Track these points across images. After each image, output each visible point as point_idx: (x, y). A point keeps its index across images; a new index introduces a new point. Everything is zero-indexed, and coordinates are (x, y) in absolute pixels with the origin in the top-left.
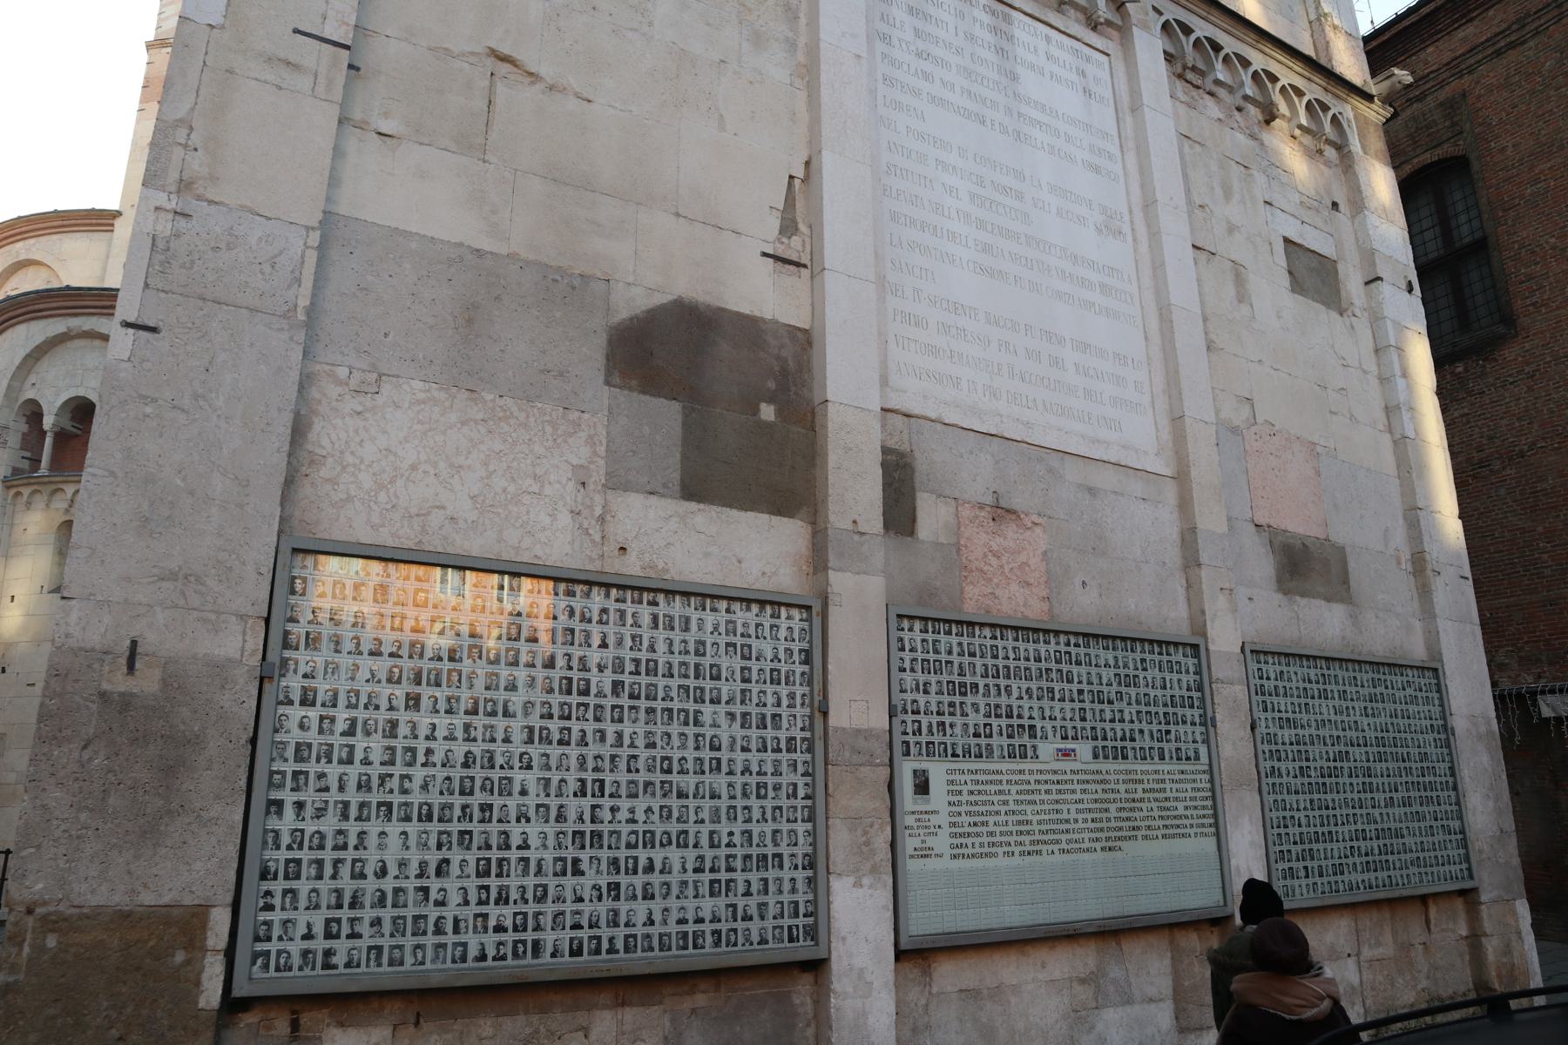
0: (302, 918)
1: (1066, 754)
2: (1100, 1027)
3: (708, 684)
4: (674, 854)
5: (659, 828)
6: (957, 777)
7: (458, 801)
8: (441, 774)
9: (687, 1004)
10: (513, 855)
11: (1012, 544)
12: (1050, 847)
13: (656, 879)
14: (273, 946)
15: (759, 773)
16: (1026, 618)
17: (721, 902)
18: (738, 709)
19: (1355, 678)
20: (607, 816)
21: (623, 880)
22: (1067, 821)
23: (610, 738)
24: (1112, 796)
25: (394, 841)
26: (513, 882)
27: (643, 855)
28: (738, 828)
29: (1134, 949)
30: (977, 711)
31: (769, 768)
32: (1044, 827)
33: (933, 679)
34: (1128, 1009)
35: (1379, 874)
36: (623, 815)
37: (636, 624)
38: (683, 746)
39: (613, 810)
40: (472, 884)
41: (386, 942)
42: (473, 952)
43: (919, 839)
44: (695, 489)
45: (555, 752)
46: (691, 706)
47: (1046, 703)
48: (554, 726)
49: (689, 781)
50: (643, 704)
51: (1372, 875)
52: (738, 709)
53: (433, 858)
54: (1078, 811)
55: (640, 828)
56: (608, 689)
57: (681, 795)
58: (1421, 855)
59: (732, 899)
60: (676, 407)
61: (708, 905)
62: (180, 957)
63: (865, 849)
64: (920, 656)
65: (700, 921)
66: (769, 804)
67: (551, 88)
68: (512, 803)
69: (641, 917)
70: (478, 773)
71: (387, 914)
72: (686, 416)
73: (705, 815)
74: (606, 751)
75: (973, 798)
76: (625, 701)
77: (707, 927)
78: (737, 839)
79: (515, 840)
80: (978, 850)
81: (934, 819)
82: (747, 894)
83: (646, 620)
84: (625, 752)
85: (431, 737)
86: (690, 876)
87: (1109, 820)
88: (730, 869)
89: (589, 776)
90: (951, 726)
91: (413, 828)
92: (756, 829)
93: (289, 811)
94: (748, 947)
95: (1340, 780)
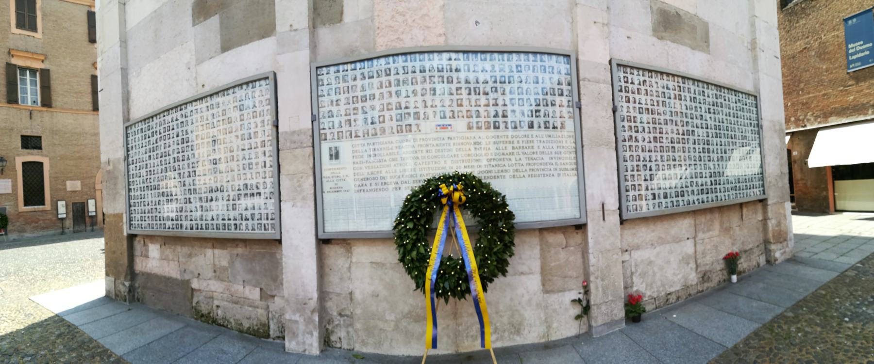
15: (249, 159)
31: (253, 156)
35: (710, 195)
51: (705, 196)
53: (157, 199)
63: (298, 189)
65: (229, 219)
80: (374, 187)
90: (355, 121)
91: (153, 192)
94: (247, 231)
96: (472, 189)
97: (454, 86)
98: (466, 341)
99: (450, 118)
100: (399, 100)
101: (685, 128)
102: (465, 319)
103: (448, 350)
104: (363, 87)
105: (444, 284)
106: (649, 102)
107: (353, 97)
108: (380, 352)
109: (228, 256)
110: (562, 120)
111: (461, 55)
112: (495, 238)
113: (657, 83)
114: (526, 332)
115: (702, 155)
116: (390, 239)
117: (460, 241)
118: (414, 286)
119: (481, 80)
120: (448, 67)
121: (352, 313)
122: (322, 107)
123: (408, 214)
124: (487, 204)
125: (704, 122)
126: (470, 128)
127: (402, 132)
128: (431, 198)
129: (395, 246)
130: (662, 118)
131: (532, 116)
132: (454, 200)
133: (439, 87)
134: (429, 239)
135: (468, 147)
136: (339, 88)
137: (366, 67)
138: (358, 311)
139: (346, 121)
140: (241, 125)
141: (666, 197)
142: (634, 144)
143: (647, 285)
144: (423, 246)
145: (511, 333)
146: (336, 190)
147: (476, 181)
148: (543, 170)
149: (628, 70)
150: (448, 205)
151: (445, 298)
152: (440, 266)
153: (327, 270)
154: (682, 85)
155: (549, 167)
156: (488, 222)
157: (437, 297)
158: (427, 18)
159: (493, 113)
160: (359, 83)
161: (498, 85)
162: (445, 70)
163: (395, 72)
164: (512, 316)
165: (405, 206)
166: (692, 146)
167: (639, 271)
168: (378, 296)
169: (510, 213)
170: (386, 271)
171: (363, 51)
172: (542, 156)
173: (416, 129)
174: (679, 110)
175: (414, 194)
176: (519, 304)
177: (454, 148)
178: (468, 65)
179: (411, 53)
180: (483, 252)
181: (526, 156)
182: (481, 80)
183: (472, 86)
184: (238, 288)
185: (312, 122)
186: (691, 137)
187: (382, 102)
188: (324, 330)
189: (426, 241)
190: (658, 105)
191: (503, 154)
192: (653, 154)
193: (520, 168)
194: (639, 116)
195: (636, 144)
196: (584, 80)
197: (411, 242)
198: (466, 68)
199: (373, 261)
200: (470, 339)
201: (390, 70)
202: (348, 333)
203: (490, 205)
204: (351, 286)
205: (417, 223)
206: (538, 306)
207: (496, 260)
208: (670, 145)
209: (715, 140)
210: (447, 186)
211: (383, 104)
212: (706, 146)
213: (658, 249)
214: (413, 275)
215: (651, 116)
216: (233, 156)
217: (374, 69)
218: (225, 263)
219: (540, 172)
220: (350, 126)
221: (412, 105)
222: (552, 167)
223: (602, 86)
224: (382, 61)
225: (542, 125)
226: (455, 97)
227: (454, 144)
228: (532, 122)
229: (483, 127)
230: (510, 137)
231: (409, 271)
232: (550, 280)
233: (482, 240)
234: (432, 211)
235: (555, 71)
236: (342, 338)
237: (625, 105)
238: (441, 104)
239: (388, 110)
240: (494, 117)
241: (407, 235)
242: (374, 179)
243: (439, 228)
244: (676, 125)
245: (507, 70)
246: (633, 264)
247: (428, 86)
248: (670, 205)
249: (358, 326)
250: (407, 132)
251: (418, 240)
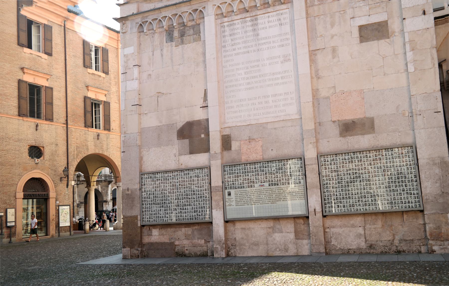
0: (147, 216)
1: (262, 186)
2: (274, 236)
3: (192, 182)
4: (189, 207)
5: (186, 204)
7: (161, 202)
8: (159, 199)
9: (194, 228)
10: (168, 208)
11: (253, 146)
12: (258, 203)
13: (186, 210)
14: (144, 220)
16: (257, 160)
17: (196, 213)
18: (197, 185)
19: (367, 155)
20: (179, 202)
21: (182, 211)
22: (262, 198)
23: (179, 192)
24: (274, 193)
25: (155, 207)
26: (168, 212)
27: (184, 207)
28: (198, 203)
29: (283, 223)
30: (241, 180)
31: (202, 194)
32: (256, 200)
33: (231, 175)
34: (281, 234)
36: (181, 202)
37: (182, 175)
38: (189, 192)
39: (180, 201)
40: (164, 212)
41: (155, 219)
42: (165, 220)
44: (192, 152)
45: (172, 194)
46: (190, 186)
47: (257, 177)
48: (172, 191)
49: (190, 197)
50: (183, 186)
52: (197, 185)
53: (159, 209)
54: (265, 196)
55: (184, 204)
56: (178, 185)
57: (189, 199)
59: (197, 213)
60: (188, 140)
61: (194, 214)
62: (136, 221)
64: (229, 172)
65: (193, 216)
66: (202, 199)
67: (166, 94)
68: (168, 202)
69: (185, 216)
70: (163, 198)
71: (155, 216)
72: (189, 141)
73: (193, 201)
74: (179, 194)
75: (240, 195)
76: (181, 186)
77: (194, 217)
78: (198, 204)
79: (168, 206)
80: (241, 204)
81: (232, 200)
82: (200, 212)
83: (183, 175)
84: (181, 193)
85: (158, 194)
86: (191, 210)
87: (273, 197)
88: (197, 209)
89: (177, 197)
91: (157, 206)
92: (200, 203)
93: (144, 205)
109: (191, 230)
133: (260, 173)
135: (269, 191)
141: (344, 207)
143: (338, 243)
155: (295, 197)
167: (334, 237)
213: (343, 229)
218: (190, 233)
222: (296, 197)
226: (265, 176)
245: (280, 165)
246: (331, 233)
247: (257, 173)
248: (346, 210)
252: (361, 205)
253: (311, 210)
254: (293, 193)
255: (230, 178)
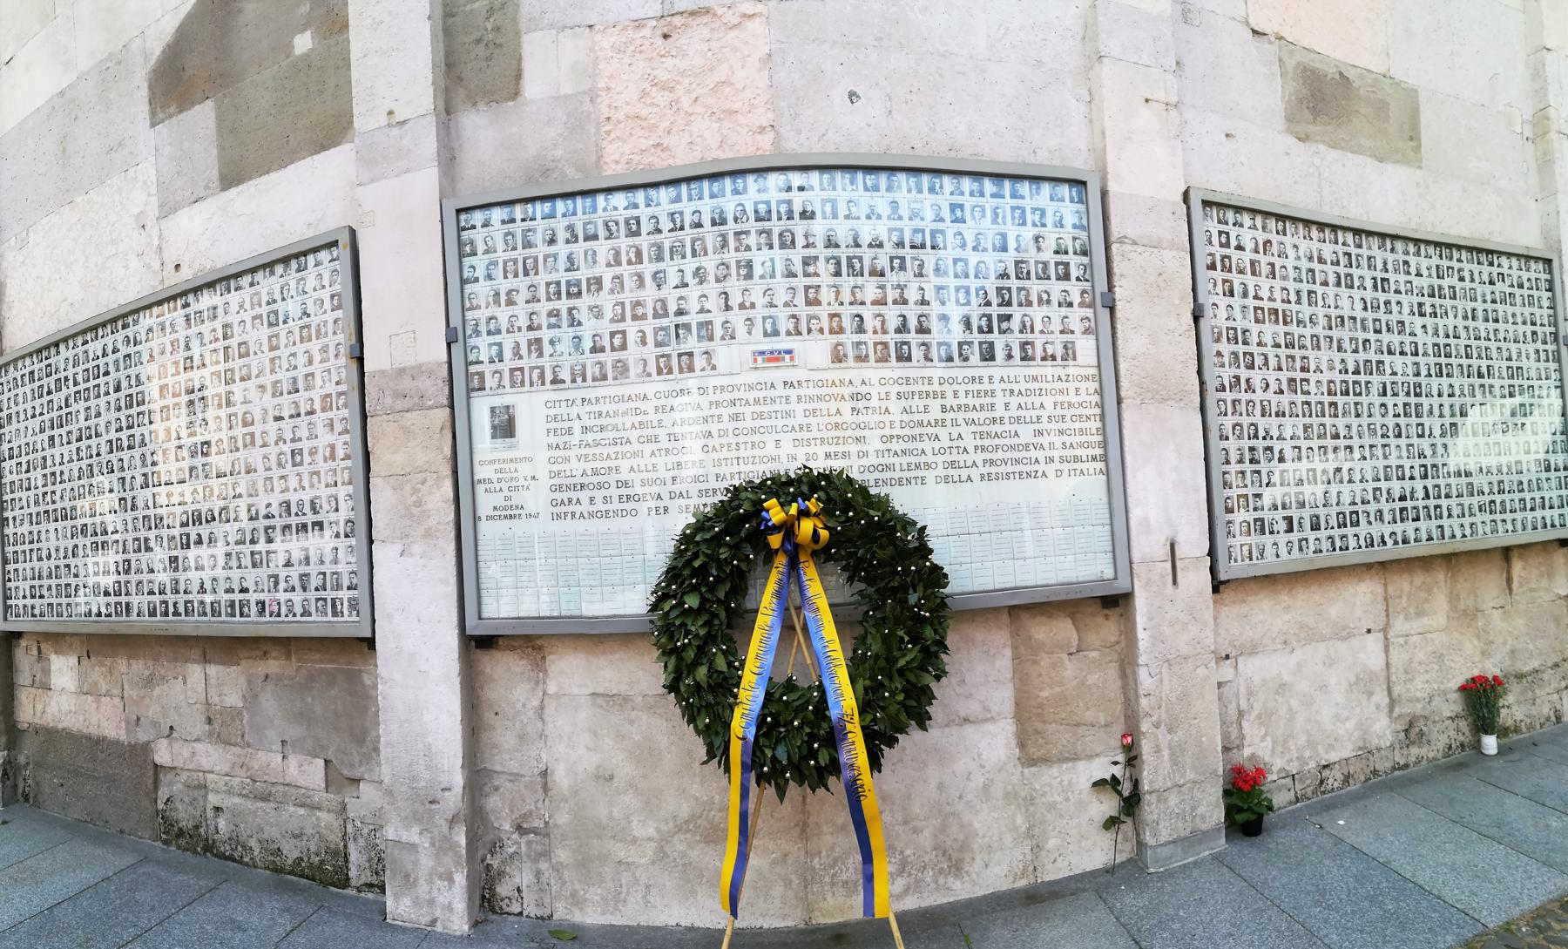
6: (563, 410)
15: (293, 440)
43: (501, 495)
58: (1498, 498)
63: (415, 511)
64: (501, 256)
65: (244, 590)
80: (600, 506)
81: (525, 470)
90: (552, 342)
94: (290, 618)
95: (1363, 399)
96: (845, 511)
97: (796, 256)
98: (829, 896)
99: (789, 333)
100: (664, 293)
101: (1361, 356)
102: (828, 839)
103: (784, 917)
104: (570, 258)
105: (774, 749)
106: (1278, 295)
107: (548, 284)
108: (617, 920)
109: (243, 681)
110: (1069, 337)
111: (814, 177)
112: (901, 633)
113: (1295, 246)
114: (978, 864)
115: (1402, 421)
116: (642, 635)
117: (817, 644)
118: (702, 752)
119: (865, 239)
120: (783, 208)
121: (546, 823)
122: (472, 308)
123: (686, 572)
124: (882, 548)
125: (1407, 339)
126: (838, 358)
127: (670, 372)
128: (743, 534)
129: (656, 653)
130: (1308, 332)
131: (990, 331)
132: (799, 540)
133: (760, 258)
134: (736, 635)
135: (833, 406)
136: (515, 262)
137: (580, 211)
138: (562, 819)
139: (530, 343)
140: (272, 360)
141: (1315, 527)
142: (1244, 397)
143: (1274, 743)
144: (725, 653)
145: (941, 871)
146: (509, 512)
147: (854, 491)
148: (1018, 461)
149: (1230, 215)
150: (785, 552)
151: (777, 786)
152: (764, 706)
153: (488, 715)
154: (1353, 251)
155: (1033, 454)
156: (883, 593)
157: (758, 783)
158: (727, 90)
159: (893, 323)
160: (562, 249)
161: (907, 252)
162: (774, 216)
163: (651, 228)
164: (943, 829)
165: (679, 553)
166: (1377, 400)
167: (1257, 707)
168: (611, 778)
169: (937, 569)
170: (633, 714)
171: (571, 172)
172: (1013, 428)
173: (704, 363)
174: (1346, 313)
175: (702, 524)
176: (961, 797)
177: (800, 409)
178: (833, 202)
179: (688, 180)
180: (872, 669)
181: (974, 428)
182: (865, 239)
183: (843, 253)
184: (269, 760)
185: (449, 345)
186: (1375, 379)
187: (620, 297)
188: (481, 868)
189: (730, 640)
190: (1298, 302)
191: (921, 424)
192: (1287, 421)
193: (961, 458)
194: (1255, 328)
195: (1249, 396)
196: (1121, 241)
197: (696, 643)
198: (828, 208)
199: (600, 690)
200: (840, 891)
201: (638, 223)
202: (538, 874)
203: (890, 550)
204: (544, 756)
205: (708, 596)
206: (1011, 797)
207: (904, 690)
208: (1327, 399)
209: (1435, 382)
210: (782, 505)
211: (623, 304)
212: (1413, 400)
213: (1298, 653)
214: (701, 726)
215: (1281, 329)
216: (252, 435)
217: (600, 217)
218: (234, 699)
219: (1009, 469)
220: (541, 355)
221: (693, 306)
222: (1040, 455)
223: (1167, 254)
224: (619, 199)
225: (1016, 353)
226: (800, 282)
227: (799, 398)
228: (991, 344)
229: (872, 357)
230: (935, 381)
231: (691, 715)
232: (1037, 732)
233: (869, 640)
234: (744, 566)
235: (1049, 220)
236: (524, 888)
237: (1223, 302)
238: (768, 299)
239: (635, 317)
240: (898, 331)
241: (683, 625)
242: (600, 486)
243: (762, 610)
244: (1340, 349)
245: (929, 215)
246: (1243, 689)
247: (731, 256)
248: (1325, 545)
249: (562, 855)
250: (681, 371)
251: (710, 639)
252: (1387, 517)
253: (1148, 546)
254: (1021, 428)
255: (510, 303)
